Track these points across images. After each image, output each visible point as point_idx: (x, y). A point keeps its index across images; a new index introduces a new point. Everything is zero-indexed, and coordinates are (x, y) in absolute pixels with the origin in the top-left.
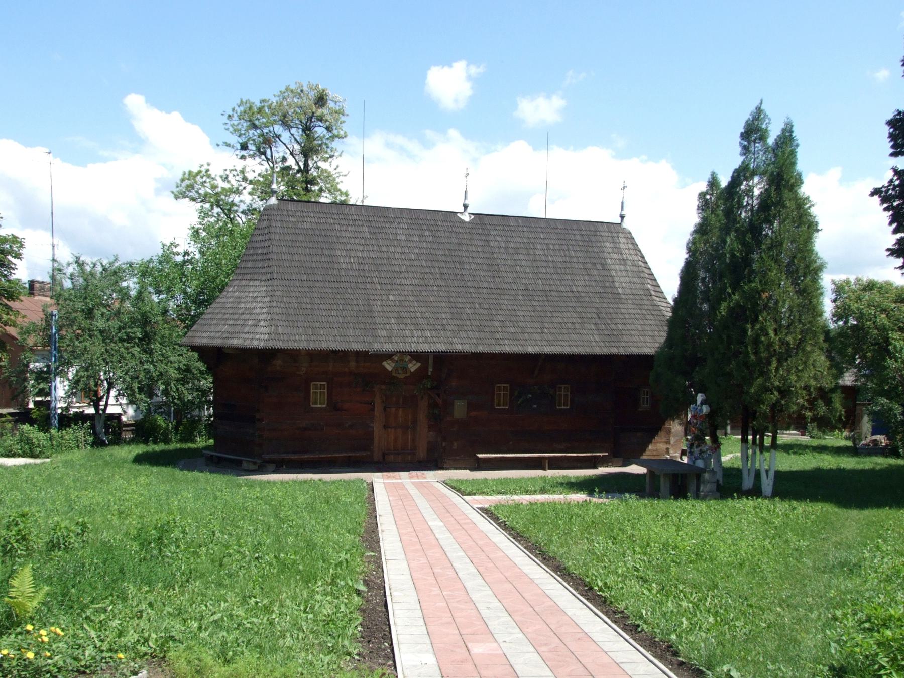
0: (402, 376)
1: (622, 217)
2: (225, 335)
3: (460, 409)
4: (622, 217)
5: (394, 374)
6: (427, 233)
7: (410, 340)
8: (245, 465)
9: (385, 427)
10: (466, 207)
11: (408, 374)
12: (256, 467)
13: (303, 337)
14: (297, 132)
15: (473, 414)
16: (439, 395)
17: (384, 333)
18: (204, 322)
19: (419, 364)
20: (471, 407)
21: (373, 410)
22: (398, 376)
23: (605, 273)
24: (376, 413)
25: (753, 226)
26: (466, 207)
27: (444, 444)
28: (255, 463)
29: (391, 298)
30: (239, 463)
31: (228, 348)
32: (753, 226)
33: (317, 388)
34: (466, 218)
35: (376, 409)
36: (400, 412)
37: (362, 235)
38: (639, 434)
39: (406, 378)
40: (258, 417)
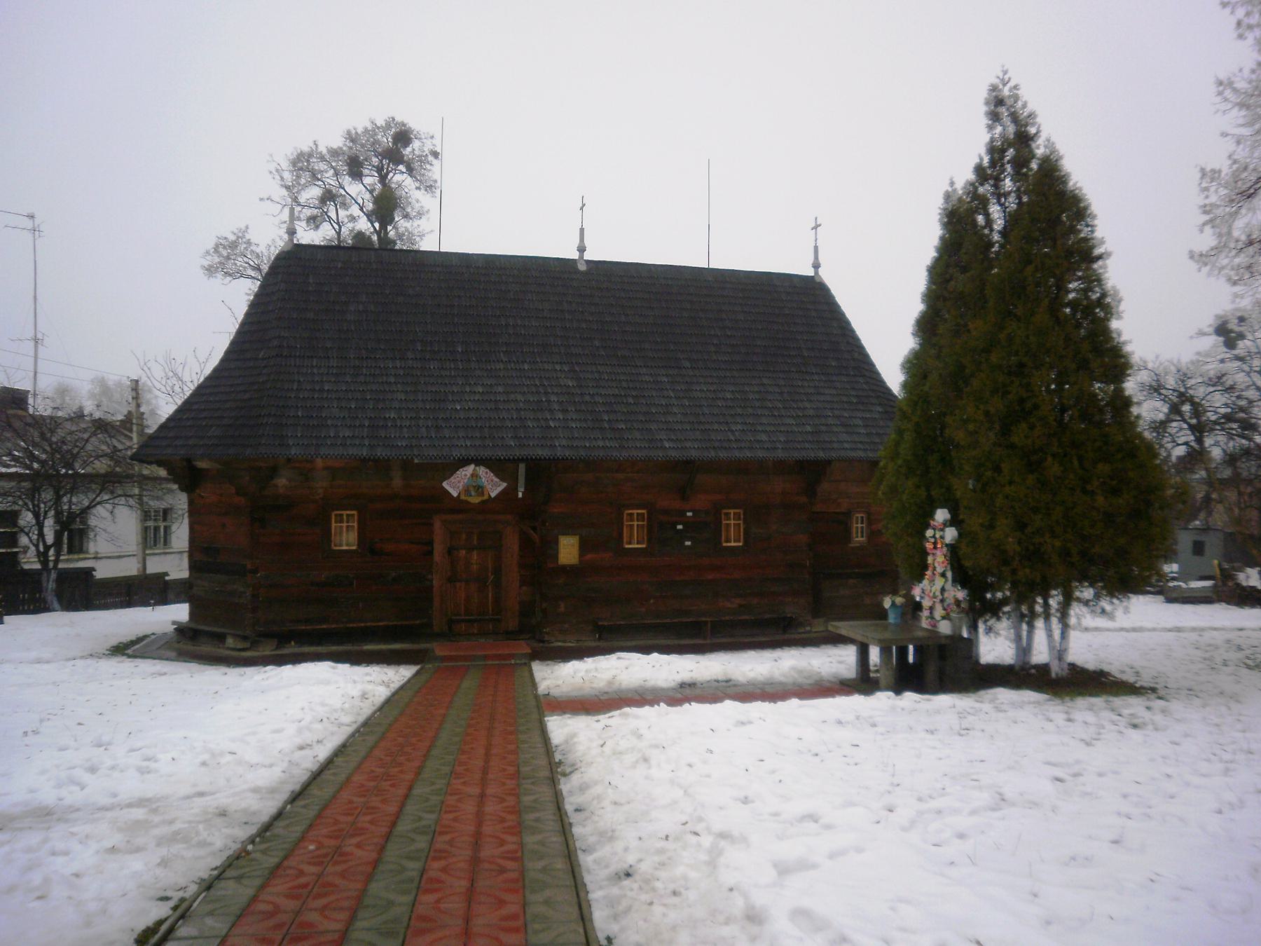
0: (475, 500)
1: (816, 266)
3: (568, 550)
4: (816, 266)
5: (463, 497)
9: (452, 579)
10: (582, 249)
11: (486, 497)
12: (247, 645)
14: (371, 179)
15: (589, 556)
16: (534, 529)
19: (505, 485)
20: (584, 547)
21: (431, 553)
22: (470, 499)
25: (1019, 253)
26: (582, 249)
27: (544, 605)
28: (245, 638)
30: (221, 638)
32: (1019, 253)
33: (341, 521)
34: (582, 267)
36: (475, 555)
38: (851, 581)
39: (483, 502)
40: (249, 567)
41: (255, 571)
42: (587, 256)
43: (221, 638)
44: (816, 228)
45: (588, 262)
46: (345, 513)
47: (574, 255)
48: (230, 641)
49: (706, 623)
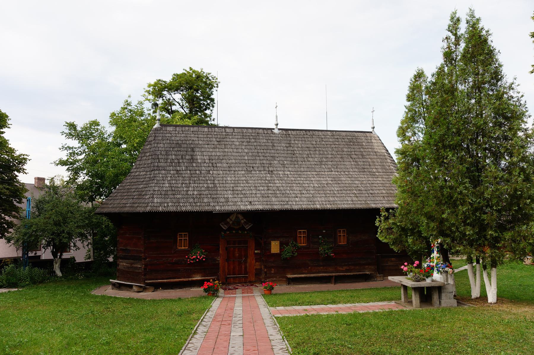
0: (237, 227)
2: (121, 206)
3: (275, 247)
6: (253, 140)
7: (240, 203)
8: (135, 288)
12: (142, 290)
13: (170, 204)
17: (222, 200)
18: (111, 198)
20: (281, 245)
23: (364, 160)
24: (221, 252)
29: (229, 179)
31: (123, 213)
34: (276, 131)
35: (220, 249)
37: (213, 143)
38: (393, 259)
41: (145, 259)
42: (279, 127)
43: (131, 287)
44: (372, 112)
45: (279, 129)
46: (183, 233)
47: (274, 127)
48: (134, 288)
49: (332, 277)
